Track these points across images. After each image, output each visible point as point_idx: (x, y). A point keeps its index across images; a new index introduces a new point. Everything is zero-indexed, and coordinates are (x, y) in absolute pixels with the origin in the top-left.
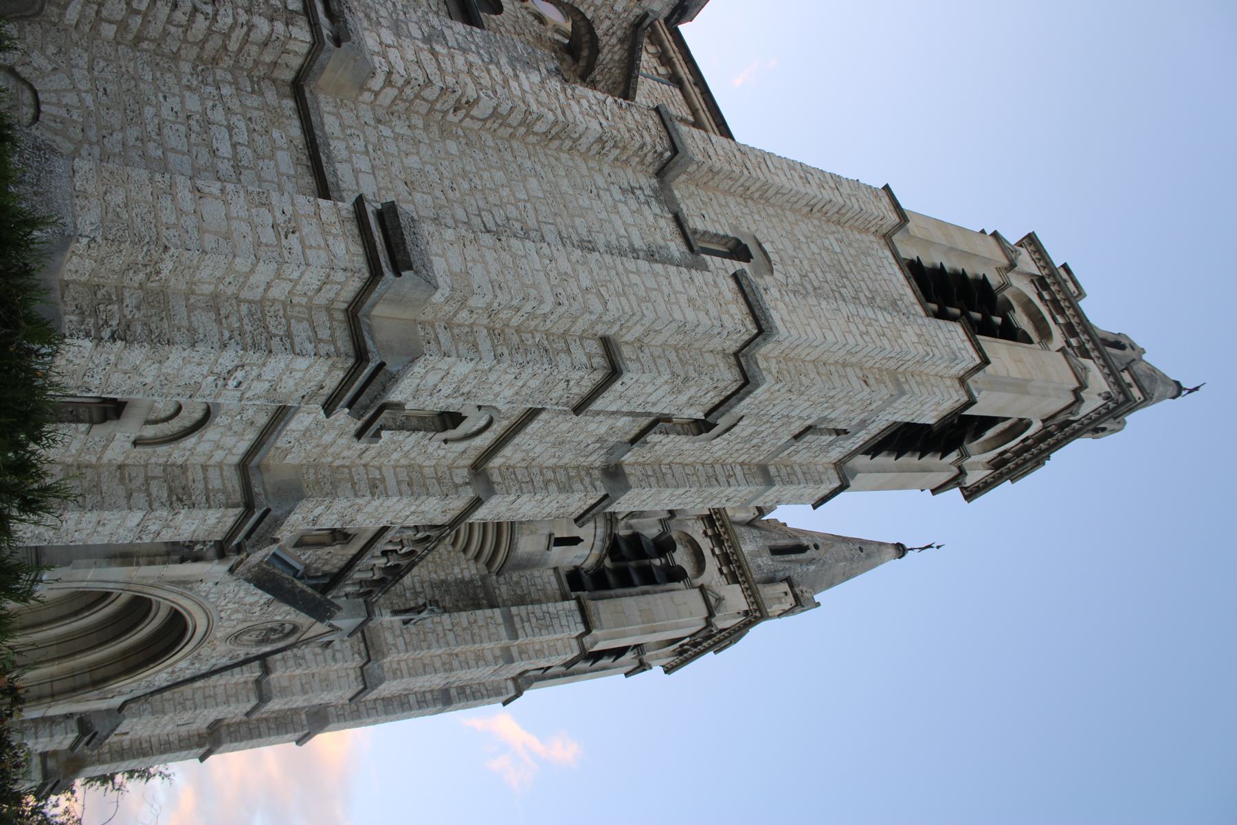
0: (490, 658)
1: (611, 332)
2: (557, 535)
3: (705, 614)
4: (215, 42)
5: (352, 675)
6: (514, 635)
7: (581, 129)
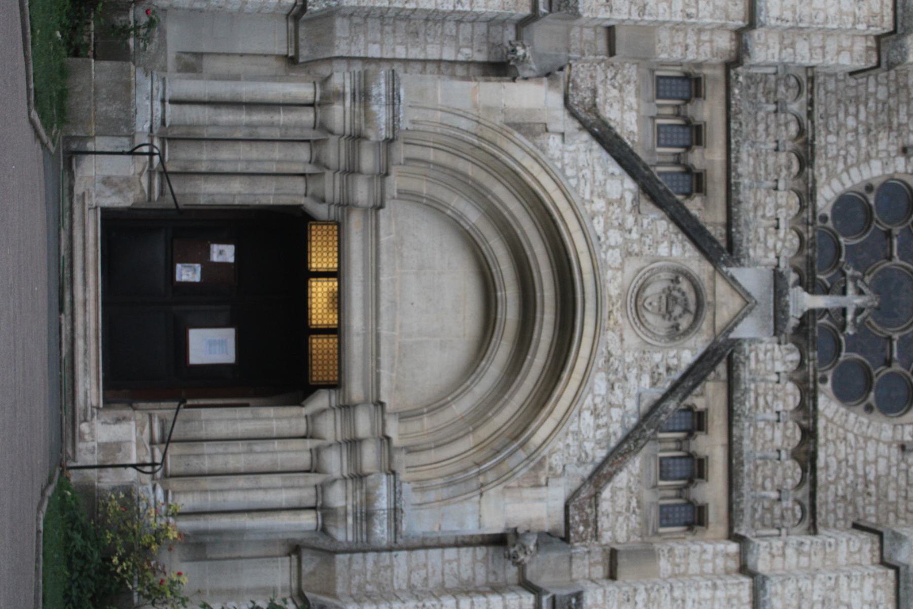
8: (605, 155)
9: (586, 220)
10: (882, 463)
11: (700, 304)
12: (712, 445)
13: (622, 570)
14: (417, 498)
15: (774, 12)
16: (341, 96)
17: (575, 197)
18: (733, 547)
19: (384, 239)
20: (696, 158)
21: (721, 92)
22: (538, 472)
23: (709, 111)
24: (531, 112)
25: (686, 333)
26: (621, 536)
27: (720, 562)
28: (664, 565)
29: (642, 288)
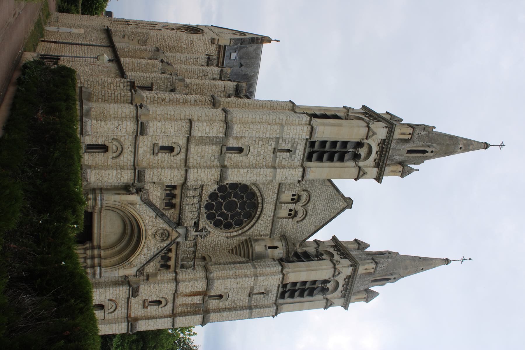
0: (249, 276)
1: (190, 118)
2: (269, 245)
3: (332, 265)
4: (116, 98)
5: (204, 278)
6: (255, 268)
7: (190, 99)
10: (222, 241)
11: (169, 235)
12: (172, 255)
14: (105, 271)
15: (192, 179)
16: (90, 199)
17: (142, 217)
18: (174, 275)
19: (102, 215)
20: (174, 201)
21: (180, 188)
22: (131, 266)
23: (177, 192)
25: (165, 240)
26: (151, 271)
27: (171, 278)
28: (159, 278)
29: (156, 233)
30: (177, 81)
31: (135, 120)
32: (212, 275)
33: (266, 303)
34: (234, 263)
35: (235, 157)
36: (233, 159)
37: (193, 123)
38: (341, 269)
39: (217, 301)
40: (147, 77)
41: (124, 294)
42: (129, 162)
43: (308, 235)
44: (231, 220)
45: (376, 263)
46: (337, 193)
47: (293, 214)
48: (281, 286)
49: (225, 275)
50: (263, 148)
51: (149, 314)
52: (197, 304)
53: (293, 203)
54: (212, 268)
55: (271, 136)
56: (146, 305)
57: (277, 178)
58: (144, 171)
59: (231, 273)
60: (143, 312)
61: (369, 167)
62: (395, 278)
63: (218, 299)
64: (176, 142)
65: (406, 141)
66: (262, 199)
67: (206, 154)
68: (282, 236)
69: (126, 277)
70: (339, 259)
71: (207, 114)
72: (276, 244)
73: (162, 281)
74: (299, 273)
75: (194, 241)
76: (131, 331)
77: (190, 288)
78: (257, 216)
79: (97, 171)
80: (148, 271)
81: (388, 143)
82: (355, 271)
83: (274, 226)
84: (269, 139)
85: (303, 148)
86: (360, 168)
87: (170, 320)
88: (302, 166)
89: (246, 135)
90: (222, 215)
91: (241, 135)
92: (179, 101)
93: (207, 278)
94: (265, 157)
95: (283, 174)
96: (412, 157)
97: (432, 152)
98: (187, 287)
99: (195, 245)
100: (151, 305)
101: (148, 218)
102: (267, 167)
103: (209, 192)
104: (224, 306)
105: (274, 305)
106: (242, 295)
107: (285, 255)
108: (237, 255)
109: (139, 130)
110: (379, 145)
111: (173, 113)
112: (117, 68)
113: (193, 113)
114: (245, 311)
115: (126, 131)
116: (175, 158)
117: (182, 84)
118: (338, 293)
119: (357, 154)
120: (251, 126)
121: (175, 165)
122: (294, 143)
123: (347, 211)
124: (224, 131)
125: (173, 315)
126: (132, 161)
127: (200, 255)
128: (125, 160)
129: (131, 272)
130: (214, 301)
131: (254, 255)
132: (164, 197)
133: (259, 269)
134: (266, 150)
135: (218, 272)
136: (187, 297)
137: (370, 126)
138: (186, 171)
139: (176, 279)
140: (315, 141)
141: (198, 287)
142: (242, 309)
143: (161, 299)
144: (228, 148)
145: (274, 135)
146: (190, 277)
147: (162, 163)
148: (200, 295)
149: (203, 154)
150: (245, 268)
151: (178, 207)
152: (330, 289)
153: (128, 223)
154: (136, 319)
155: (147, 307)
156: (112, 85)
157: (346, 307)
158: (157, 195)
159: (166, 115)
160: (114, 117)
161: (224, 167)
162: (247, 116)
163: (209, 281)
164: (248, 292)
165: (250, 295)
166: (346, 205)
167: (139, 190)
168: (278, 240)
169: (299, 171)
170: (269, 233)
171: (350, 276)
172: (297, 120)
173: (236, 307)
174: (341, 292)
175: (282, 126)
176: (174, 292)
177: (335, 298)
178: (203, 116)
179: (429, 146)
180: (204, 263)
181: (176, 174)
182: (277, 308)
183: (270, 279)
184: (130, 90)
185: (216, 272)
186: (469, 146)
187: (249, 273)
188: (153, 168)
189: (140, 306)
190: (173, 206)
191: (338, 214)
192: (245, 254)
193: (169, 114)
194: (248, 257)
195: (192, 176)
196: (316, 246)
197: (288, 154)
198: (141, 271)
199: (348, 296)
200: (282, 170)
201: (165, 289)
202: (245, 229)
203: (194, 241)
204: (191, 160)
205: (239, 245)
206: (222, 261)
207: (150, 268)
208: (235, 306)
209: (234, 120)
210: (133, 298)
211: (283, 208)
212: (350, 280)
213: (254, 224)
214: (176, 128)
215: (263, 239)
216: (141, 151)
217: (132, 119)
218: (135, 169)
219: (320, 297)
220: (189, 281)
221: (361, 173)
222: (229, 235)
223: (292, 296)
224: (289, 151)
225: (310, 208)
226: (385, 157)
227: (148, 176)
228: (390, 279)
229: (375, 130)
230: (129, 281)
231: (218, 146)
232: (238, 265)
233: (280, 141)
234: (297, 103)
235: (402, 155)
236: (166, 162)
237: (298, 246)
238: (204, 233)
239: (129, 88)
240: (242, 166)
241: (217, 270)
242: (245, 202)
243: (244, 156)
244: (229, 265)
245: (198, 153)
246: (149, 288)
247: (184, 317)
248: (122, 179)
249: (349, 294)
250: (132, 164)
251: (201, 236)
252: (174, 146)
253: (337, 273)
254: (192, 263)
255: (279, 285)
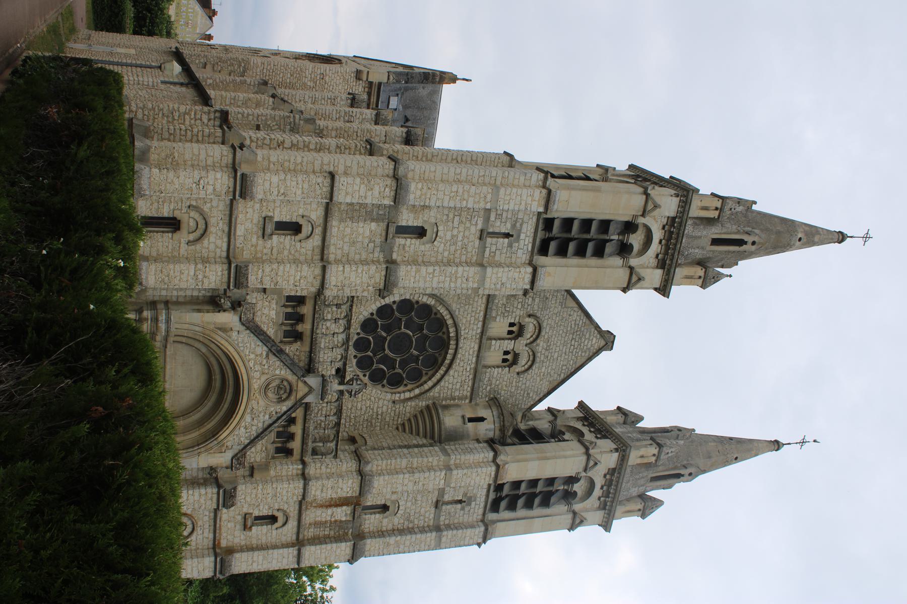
0: (436, 468)
1: (332, 169)
2: (469, 415)
3: (583, 450)
5: (355, 473)
6: (446, 454)
8: (256, 338)
9: (246, 362)
10: (385, 408)
11: (291, 390)
12: (297, 429)
13: (255, 475)
15: (333, 283)
17: (243, 355)
18: (300, 467)
19: (168, 353)
20: (300, 328)
21: (312, 302)
23: (306, 310)
24: (225, 324)
25: (285, 400)
26: (258, 459)
27: (295, 472)
28: (272, 473)
29: (268, 385)
30: (302, 122)
31: (230, 170)
32: (368, 468)
33: (466, 520)
34: (408, 447)
35: (411, 244)
36: (407, 249)
37: (337, 177)
38: (598, 457)
39: (377, 516)
40: (248, 115)
41: (209, 502)
42: (218, 251)
43: (537, 398)
44: (400, 371)
45: (660, 446)
46: (588, 322)
47: (510, 360)
48: (492, 488)
49: (393, 467)
50: (461, 229)
51: (254, 542)
52: (341, 521)
53: (510, 339)
54: (368, 455)
55: (476, 206)
56: (249, 523)
57: (487, 285)
58: (247, 266)
59: (404, 462)
60: (243, 537)
61: (647, 267)
62: (690, 474)
63: (379, 513)
64: (305, 214)
65: (710, 221)
66: (457, 331)
67: (360, 239)
68: (492, 399)
69: (212, 469)
70: (594, 440)
71: (362, 163)
72: (482, 413)
73: (279, 479)
74: (525, 465)
75: (336, 404)
76: (221, 573)
77: (330, 492)
78: (447, 362)
79: (159, 265)
80: (252, 460)
81: (680, 223)
82: (623, 459)
83: (477, 380)
84: (471, 212)
85: (533, 230)
86: (631, 268)
87: (293, 551)
88: (530, 263)
89: (432, 204)
90: (385, 360)
91: (422, 204)
92: (308, 147)
93: (360, 472)
94: (464, 247)
95: (497, 278)
96: (720, 252)
97: (754, 243)
98: (325, 489)
99: (339, 412)
100: (257, 525)
101: (252, 356)
102: (469, 264)
103: (361, 316)
104: (390, 527)
105: (480, 523)
106: (424, 504)
107: (497, 433)
108: (412, 433)
109: (238, 188)
110: (664, 228)
111: (299, 160)
112: (195, 94)
113: (336, 161)
114: (429, 534)
115: (214, 190)
116: (303, 244)
117: (311, 127)
118: (593, 501)
119: (626, 244)
120: (441, 186)
121: (302, 258)
122: (516, 222)
123: (604, 354)
124: (393, 193)
125: (299, 543)
126: (225, 248)
127: (345, 434)
128: (212, 247)
129: (221, 459)
130: (373, 516)
131: (443, 433)
132: (281, 319)
133: (453, 457)
134: (467, 233)
135: (380, 462)
136: (324, 510)
137: (649, 192)
138: (324, 269)
139: (303, 474)
140: (554, 219)
141: (345, 490)
142: (423, 530)
143: (276, 514)
144: (399, 229)
145: (482, 205)
146: (329, 470)
147: (278, 253)
148: (347, 505)
149: (354, 237)
150: (429, 454)
151: (307, 339)
152: (579, 493)
153: (216, 368)
154: (230, 551)
155: (251, 527)
156: (187, 117)
157: (607, 526)
158: (269, 315)
159: (286, 164)
160: (193, 166)
161: (391, 265)
162: (433, 169)
163: (364, 478)
164: (435, 500)
165: (437, 505)
166: (603, 343)
167: (236, 305)
168: (485, 407)
169: (526, 273)
170: (469, 394)
171: (614, 470)
172: (522, 178)
173: (413, 528)
174: (599, 499)
175: (496, 188)
176: (300, 498)
177: (587, 510)
178: (355, 167)
179: (748, 233)
180: (352, 448)
181: (304, 274)
182: (486, 529)
183: (474, 474)
184: (221, 127)
185: (376, 463)
186: (813, 236)
187: (435, 463)
188: (263, 262)
189: (238, 527)
190: (297, 336)
191: (590, 359)
192: (427, 430)
193: (292, 160)
194: (432, 437)
195: (333, 278)
196: (550, 418)
197: (506, 240)
198: (239, 458)
199: (611, 506)
200: (495, 270)
201: (284, 492)
202: (426, 387)
203: (336, 404)
204: (332, 249)
205: (415, 416)
206: (385, 445)
207: (256, 455)
208: (411, 525)
209: (410, 175)
210: (225, 510)
211: (493, 348)
212: (614, 475)
213: (443, 377)
214: (306, 186)
215: (457, 406)
216: (240, 231)
217: (225, 169)
218: (230, 264)
219: (562, 508)
220: (328, 478)
221: (634, 278)
222: (397, 397)
223: (512, 507)
224: (507, 235)
225: (540, 349)
226: (674, 249)
227: (254, 278)
228: (683, 475)
229: (658, 200)
230: (216, 479)
231: (381, 224)
232: (416, 450)
233: (492, 218)
234: (518, 157)
235: (703, 248)
236: (286, 253)
237: (519, 419)
238: (355, 387)
239: (217, 123)
240: (423, 262)
241: (379, 458)
242: (426, 337)
243: (427, 243)
244: (399, 450)
245: (344, 236)
246: (254, 491)
247: (318, 547)
248: (206, 281)
249: (612, 502)
250: (224, 254)
251: (350, 393)
252: (301, 221)
253: (591, 463)
254: (332, 445)
255: (489, 485)
